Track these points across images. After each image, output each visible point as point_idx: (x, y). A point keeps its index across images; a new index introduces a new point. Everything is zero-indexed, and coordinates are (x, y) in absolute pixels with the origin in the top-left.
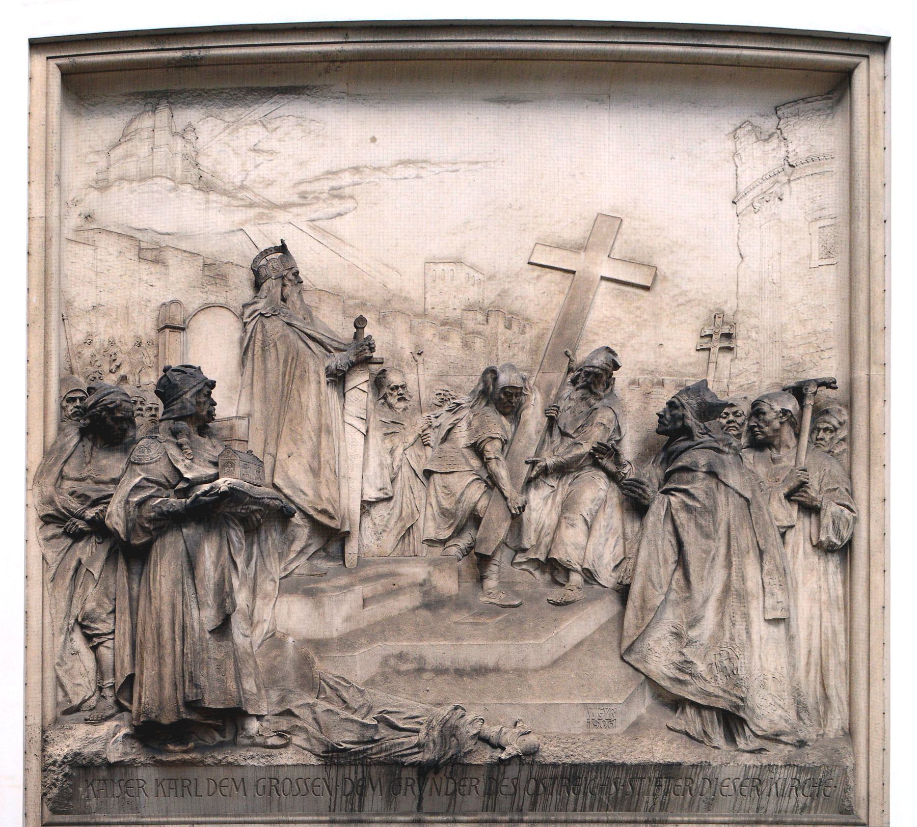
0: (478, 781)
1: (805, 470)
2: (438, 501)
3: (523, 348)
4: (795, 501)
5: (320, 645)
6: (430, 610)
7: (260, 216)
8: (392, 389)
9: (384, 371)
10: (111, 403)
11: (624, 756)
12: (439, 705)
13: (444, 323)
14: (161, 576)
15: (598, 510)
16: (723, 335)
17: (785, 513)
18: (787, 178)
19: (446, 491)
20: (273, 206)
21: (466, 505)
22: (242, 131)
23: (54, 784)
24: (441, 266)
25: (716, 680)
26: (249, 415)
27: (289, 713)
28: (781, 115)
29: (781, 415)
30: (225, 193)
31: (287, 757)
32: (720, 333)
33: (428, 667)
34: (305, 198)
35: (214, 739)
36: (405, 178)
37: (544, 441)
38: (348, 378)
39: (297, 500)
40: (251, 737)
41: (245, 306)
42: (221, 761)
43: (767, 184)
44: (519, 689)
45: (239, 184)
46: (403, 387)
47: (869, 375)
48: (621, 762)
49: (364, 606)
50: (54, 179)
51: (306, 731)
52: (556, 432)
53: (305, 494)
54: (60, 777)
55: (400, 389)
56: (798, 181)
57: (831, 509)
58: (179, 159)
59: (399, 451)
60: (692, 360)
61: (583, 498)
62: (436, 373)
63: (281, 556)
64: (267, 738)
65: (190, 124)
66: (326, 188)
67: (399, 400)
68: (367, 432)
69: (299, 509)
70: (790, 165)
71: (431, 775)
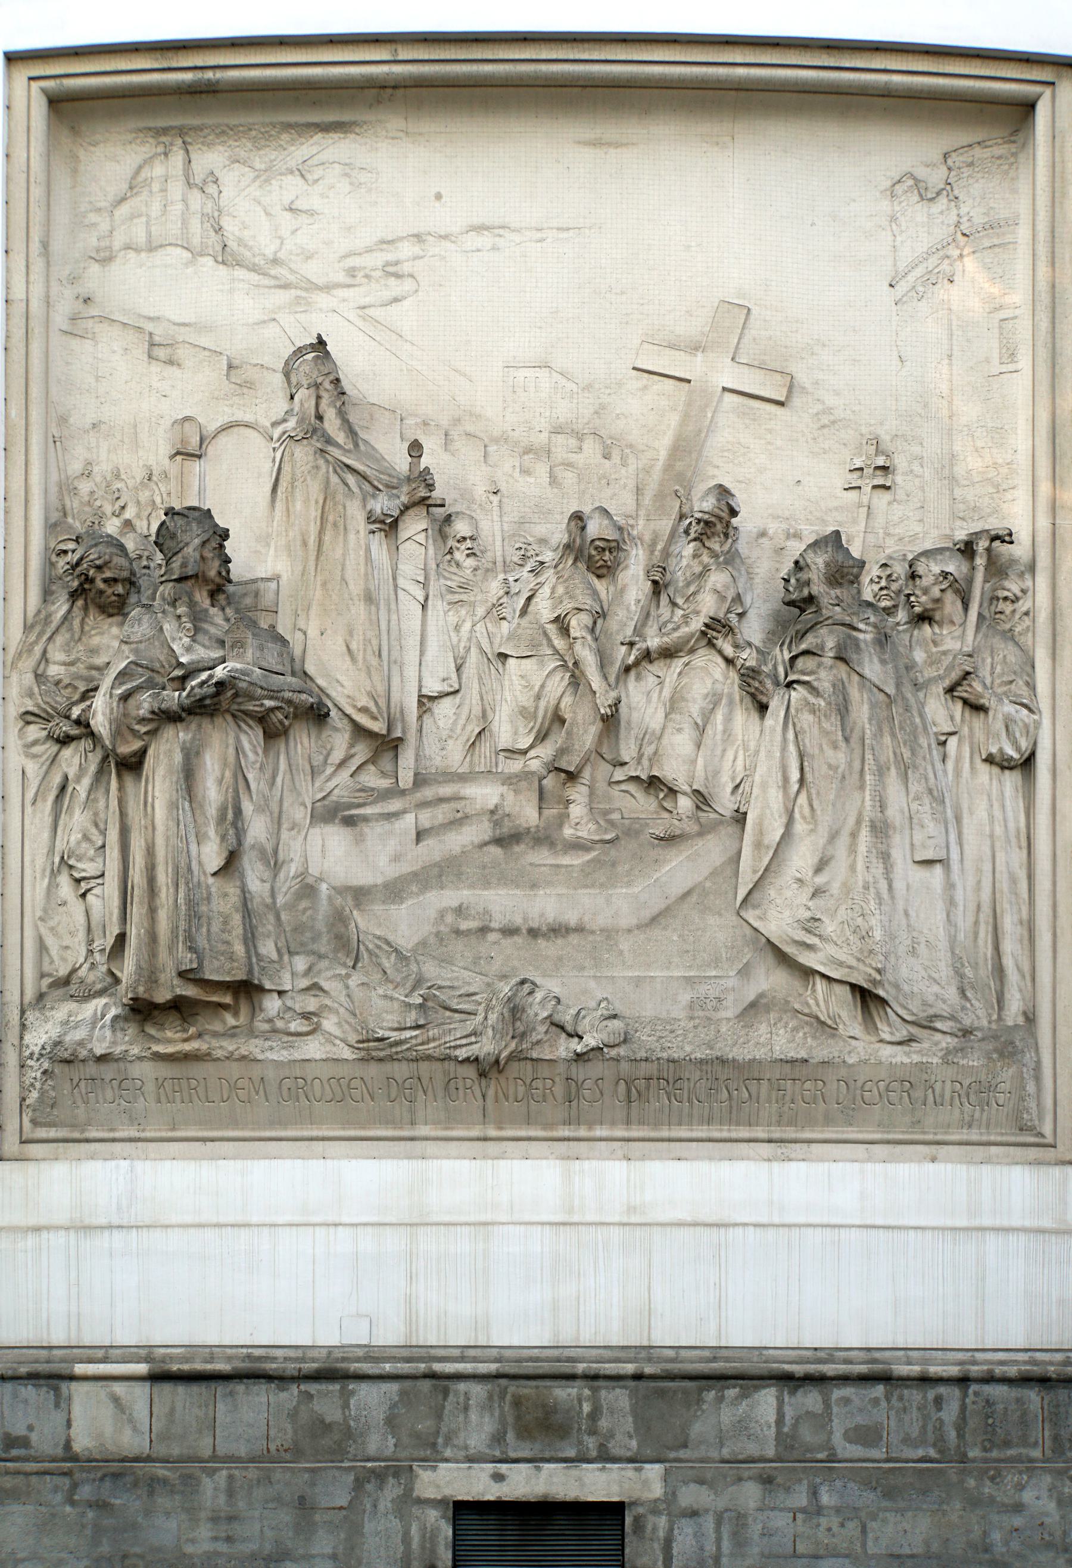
5: (360, 895)
6: (502, 846)
9: (450, 516)
13: (528, 451)
16: (877, 468)
19: (523, 682)
20: (314, 287)
23: (32, 1085)
30: (254, 269)
31: (313, 1049)
33: (494, 925)
34: (354, 276)
35: (224, 1022)
37: (648, 614)
38: (401, 525)
39: (333, 694)
40: (270, 1021)
41: (275, 424)
42: (232, 1053)
45: (271, 257)
46: (471, 538)
50: (35, 246)
52: (664, 599)
54: (39, 1074)
66: (380, 264)
68: (426, 599)
70: (964, 235)
71: (494, 1074)
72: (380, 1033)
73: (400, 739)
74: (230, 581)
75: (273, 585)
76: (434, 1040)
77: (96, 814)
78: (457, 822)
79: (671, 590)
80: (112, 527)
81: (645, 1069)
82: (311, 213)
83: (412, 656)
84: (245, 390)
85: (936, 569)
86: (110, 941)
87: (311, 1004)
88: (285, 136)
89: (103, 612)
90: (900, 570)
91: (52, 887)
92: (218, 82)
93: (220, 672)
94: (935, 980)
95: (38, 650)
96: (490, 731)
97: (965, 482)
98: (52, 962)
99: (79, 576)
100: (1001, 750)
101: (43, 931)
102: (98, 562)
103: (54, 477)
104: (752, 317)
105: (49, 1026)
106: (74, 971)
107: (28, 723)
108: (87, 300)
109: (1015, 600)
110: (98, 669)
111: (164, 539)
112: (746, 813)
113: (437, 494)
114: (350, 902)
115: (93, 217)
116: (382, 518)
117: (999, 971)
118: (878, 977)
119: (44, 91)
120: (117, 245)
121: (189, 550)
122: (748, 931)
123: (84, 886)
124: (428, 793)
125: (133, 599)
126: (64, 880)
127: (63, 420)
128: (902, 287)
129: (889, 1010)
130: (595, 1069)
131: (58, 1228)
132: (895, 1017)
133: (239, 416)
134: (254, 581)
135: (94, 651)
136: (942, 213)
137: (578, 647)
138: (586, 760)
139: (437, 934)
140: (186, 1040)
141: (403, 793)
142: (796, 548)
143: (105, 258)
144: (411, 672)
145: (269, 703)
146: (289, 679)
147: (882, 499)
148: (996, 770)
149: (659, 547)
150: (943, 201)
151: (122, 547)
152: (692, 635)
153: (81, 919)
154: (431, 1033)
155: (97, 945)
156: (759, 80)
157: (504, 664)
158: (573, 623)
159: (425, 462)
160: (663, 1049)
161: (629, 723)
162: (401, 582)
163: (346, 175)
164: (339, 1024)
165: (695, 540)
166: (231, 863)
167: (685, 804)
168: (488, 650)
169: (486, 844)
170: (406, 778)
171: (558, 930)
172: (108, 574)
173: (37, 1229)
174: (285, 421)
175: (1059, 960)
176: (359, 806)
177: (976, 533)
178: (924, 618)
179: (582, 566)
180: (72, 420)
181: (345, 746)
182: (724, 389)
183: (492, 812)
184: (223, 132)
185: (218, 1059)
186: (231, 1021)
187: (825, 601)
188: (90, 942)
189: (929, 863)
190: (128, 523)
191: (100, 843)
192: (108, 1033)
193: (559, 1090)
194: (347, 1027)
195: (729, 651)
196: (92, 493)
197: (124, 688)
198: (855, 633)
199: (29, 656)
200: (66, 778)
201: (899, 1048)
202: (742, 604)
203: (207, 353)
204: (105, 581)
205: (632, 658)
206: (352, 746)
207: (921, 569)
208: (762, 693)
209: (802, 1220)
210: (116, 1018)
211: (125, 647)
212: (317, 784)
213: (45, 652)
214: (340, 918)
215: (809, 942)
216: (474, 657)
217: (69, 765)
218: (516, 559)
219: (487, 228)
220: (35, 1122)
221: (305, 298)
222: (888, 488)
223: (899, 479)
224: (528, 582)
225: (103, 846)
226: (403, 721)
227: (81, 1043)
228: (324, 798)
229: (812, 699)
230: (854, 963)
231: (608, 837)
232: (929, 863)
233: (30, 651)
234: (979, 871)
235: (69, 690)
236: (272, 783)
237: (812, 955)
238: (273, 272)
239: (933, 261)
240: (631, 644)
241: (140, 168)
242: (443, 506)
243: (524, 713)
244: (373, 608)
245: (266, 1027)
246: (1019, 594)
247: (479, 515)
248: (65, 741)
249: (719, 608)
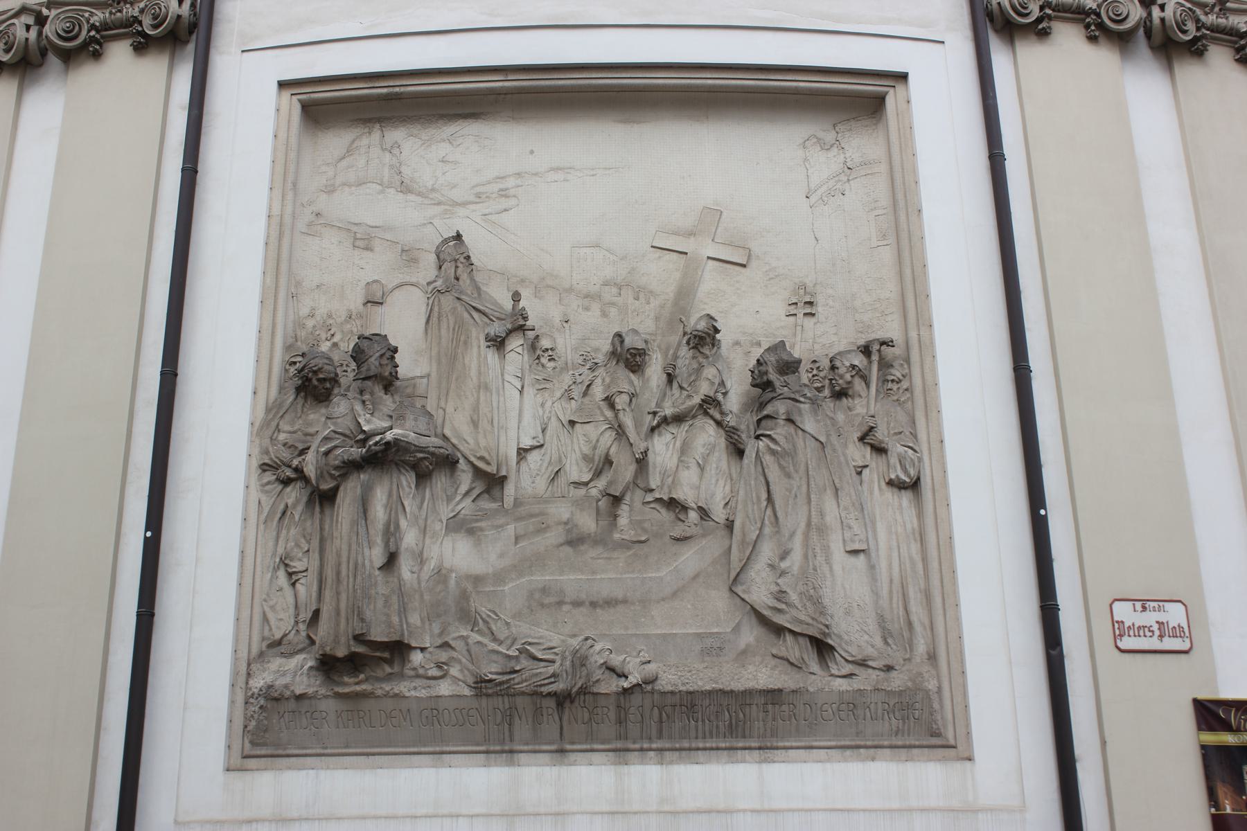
0: (609, 709)
1: (873, 417)
2: (580, 447)
3: (648, 316)
4: (868, 443)
5: (477, 580)
6: (572, 546)
7: (446, 212)
8: (543, 351)
9: (538, 336)
10: (316, 366)
11: (732, 683)
12: (574, 636)
13: (587, 296)
14: (342, 517)
15: (709, 454)
16: (806, 303)
17: (861, 454)
18: (846, 178)
19: (585, 439)
20: (456, 204)
21: (600, 451)
22: (434, 147)
23: (252, 716)
24: (585, 250)
25: (806, 609)
26: (428, 376)
27: (446, 645)
28: (839, 130)
29: (851, 369)
30: (419, 194)
31: (444, 688)
32: (803, 301)
33: (567, 599)
34: (480, 197)
35: (384, 670)
36: (557, 181)
37: (665, 395)
38: (507, 342)
39: (462, 448)
40: (415, 669)
41: (429, 284)
42: (388, 692)
43: (831, 183)
44: (643, 620)
45: (430, 187)
46: (552, 349)
47: (919, 335)
48: (729, 689)
49: (516, 543)
50: (290, 185)
51: (460, 662)
52: (675, 385)
53: (468, 443)
54: (257, 709)
55: (550, 351)
56: (856, 180)
57: (896, 449)
58: (386, 170)
59: (549, 404)
60: (782, 324)
61: (695, 444)
62: (580, 337)
63: (449, 499)
64: (428, 669)
65: (396, 142)
66: (496, 189)
67: (549, 360)
68: (523, 387)
69: (463, 455)
70: (849, 168)
71: (567, 704)
73: (505, 478)
74: (397, 379)
75: (425, 380)
76: (526, 681)
77: (304, 529)
78: (542, 529)
79: (679, 379)
80: (325, 347)
81: (670, 700)
82: (455, 163)
83: (513, 424)
84: (412, 264)
85: (848, 364)
86: (310, 615)
88: (441, 122)
89: (317, 400)
90: (826, 363)
91: (274, 577)
92: (402, 93)
93: (389, 436)
94: (865, 632)
95: (274, 424)
96: (565, 472)
97: (860, 311)
98: (271, 630)
99: (302, 378)
100: (897, 476)
101: (267, 609)
102: (314, 369)
103: (291, 317)
104: (723, 217)
105: (265, 675)
106: (285, 635)
107: (264, 471)
108: (318, 214)
109: (899, 381)
110: (312, 435)
111: (358, 355)
112: (733, 521)
115: (324, 168)
116: (495, 338)
117: (910, 624)
118: (827, 631)
119: (300, 101)
120: (337, 183)
121: (372, 359)
123: (294, 578)
125: (336, 391)
126: (281, 574)
127: (298, 284)
128: (813, 199)
129: (836, 653)
130: (636, 699)
131: (263, 820)
132: (840, 658)
133: (408, 279)
134: (413, 378)
135: (310, 424)
136: (835, 156)
137: (621, 415)
138: (626, 489)
140: (357, 684)
142: (757, 353)
143: (330, 190)
144: (513, 434)
145: (421, 455)
146: (433, 439)
147: (809, 322)
148: (896, 490)
149: (671, 352)
150: (835, 150)
151: (329, 359)
152: (694, 407)
153: (291, 600)
154: (524, 676)
155: (302, 617)
156: (721, 86)
157: (573, 427)
158: (617, 400)
159: (522, 304)
160: (683, 684)
161: (654, 464)
162: (507, 377)
163: (477, 141)
164: (461, 671)
165: (693, 348)
166: (391, 560)
167: (693, 516)
168: (562, 420)
169: (562, 545)
172: (321, 376)
173: (249, 822)
174: (435, 281)
175: (948, 616)
176: (477, 521)
177: (871, 341)
179: (622, 365)
180: (304, 284)
181: (469, 481)
182: (709, 258)
183: (566, 523)
184: (404, 120)
185: (379, 696)
186: (388, 670)
187: (777, 384)
188: (297, 615)
189: (855, 552)
190: (335, 345)
191: (306, 549)
192: (305, 679)
193: (612, 715)
194: (466, 672)
195: (718, 416)
196: (314, 327)
197: (326, 447)
198: (798, 404)
199: (267, 428)
200: (287, 506)
201: (845, 679)
202: (725, 387)
203: (389, 243)
204: (319, 380)
205: (656, 422)
206: (473, 482)
207: (838, 364)
208: (740, 443)
210: (311, 668)
211: (329, 421)
212: (450, 508)
213: (278, 425)
214: (464, 596)
215: (779, 607)
216: (554, 423)
217: (289, 498)
218: (580, 362)
219: (561, 169)
220: (252, 743)
221: (450, 210)
222: (813, 315)
223: (820, 309)
224: (588, 375)
225: (308, 551)
226: (507, 465)
227: (286, 686)
228: (454, 516)
229: (772, 446)
230: (811, 621)
232: (855, 552)
235: (292, 449)
236: (420, 508)
237: (782, 616)
238: (431, 196)
239: (831, 183)
240: (655, 413)
241: (354, 141)
242: (534, 330)
243: (587, 458)
244: (488, 394)
245: (412, 673)
246: (901, 378)
247: (557, 335)
248: (286, 482)
249: (711, 390)
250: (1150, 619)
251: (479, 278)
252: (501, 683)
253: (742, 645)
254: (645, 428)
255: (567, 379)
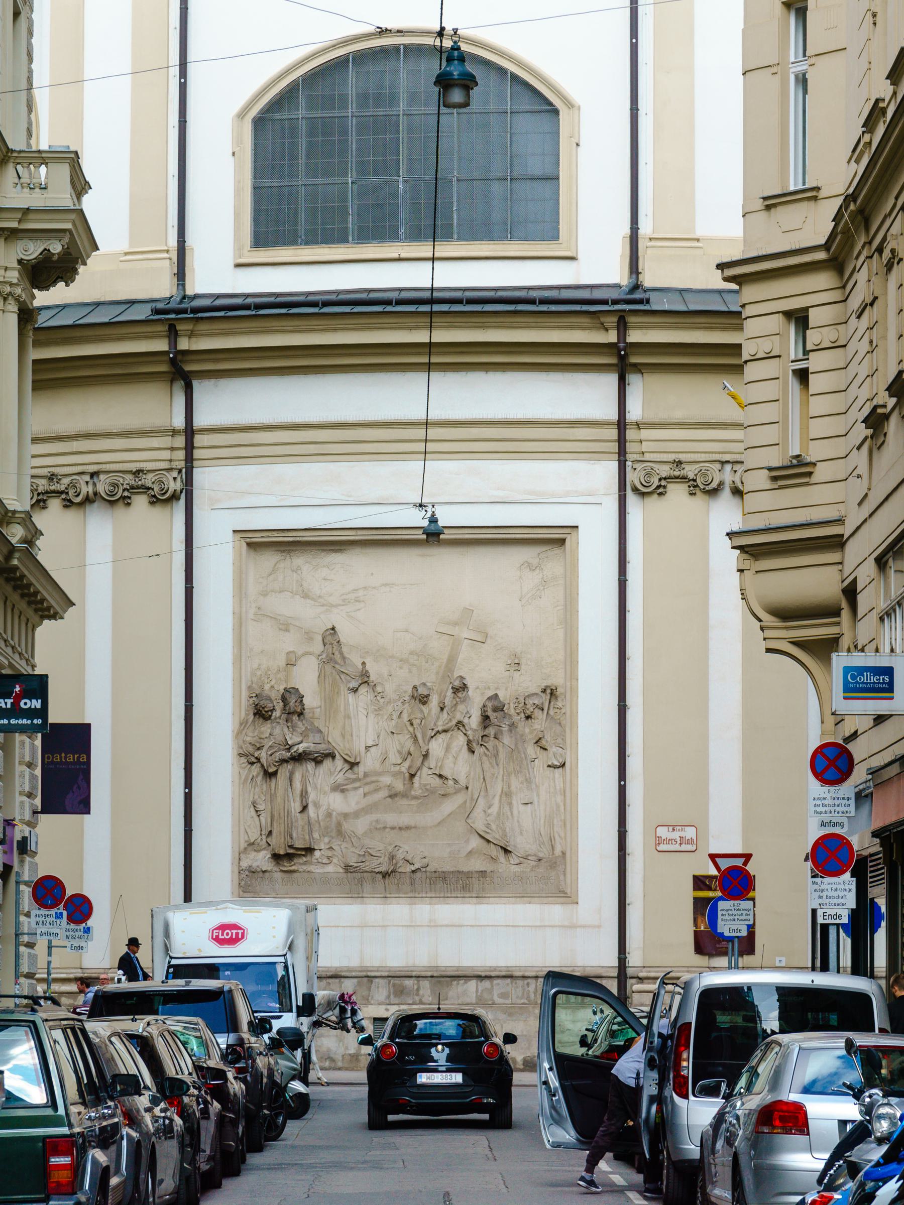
5: (346, 816)
20: (332, 606)
26: (320, 707)
30: (313, 599)
33: (388, 826)
59: (380, 723)
71: (387, 877)
72: (351, 864)
73: (359, 762)
75: (319, 710)
78: (376, 790)
82: (331, 580)
87: (330, 853)
109: (561, 709)
113: (372, 678)
114: (343, 819)
122: (469, 827)
123: (259, 813)
124: (368, 780)
130: (418, 875)
134: (313, 708)
135: (262, 733)
139: (370, 829)
141: (360, 780)
150: (537, 571)
155: (263, 832)
167: (451, 782)
170: (361, 775)
171: (408, 828)
178: (528, 717)
183: (389, 786)
193: (408, 881)
195: (464, 731)
209: (485, 924)
214: (339, 824)
216: (383, 733)
227: (258, 866)
231: (426, 794)
233: (241, 732)
234: (546, 804)
241: (275, 565)
243: (400, 752)
248: (252, 763)
250: (676, 835)
251: (345, 650)
252: (356, 867)
253: (469, 849)
254: (428, 737)
255: (390, 708)
